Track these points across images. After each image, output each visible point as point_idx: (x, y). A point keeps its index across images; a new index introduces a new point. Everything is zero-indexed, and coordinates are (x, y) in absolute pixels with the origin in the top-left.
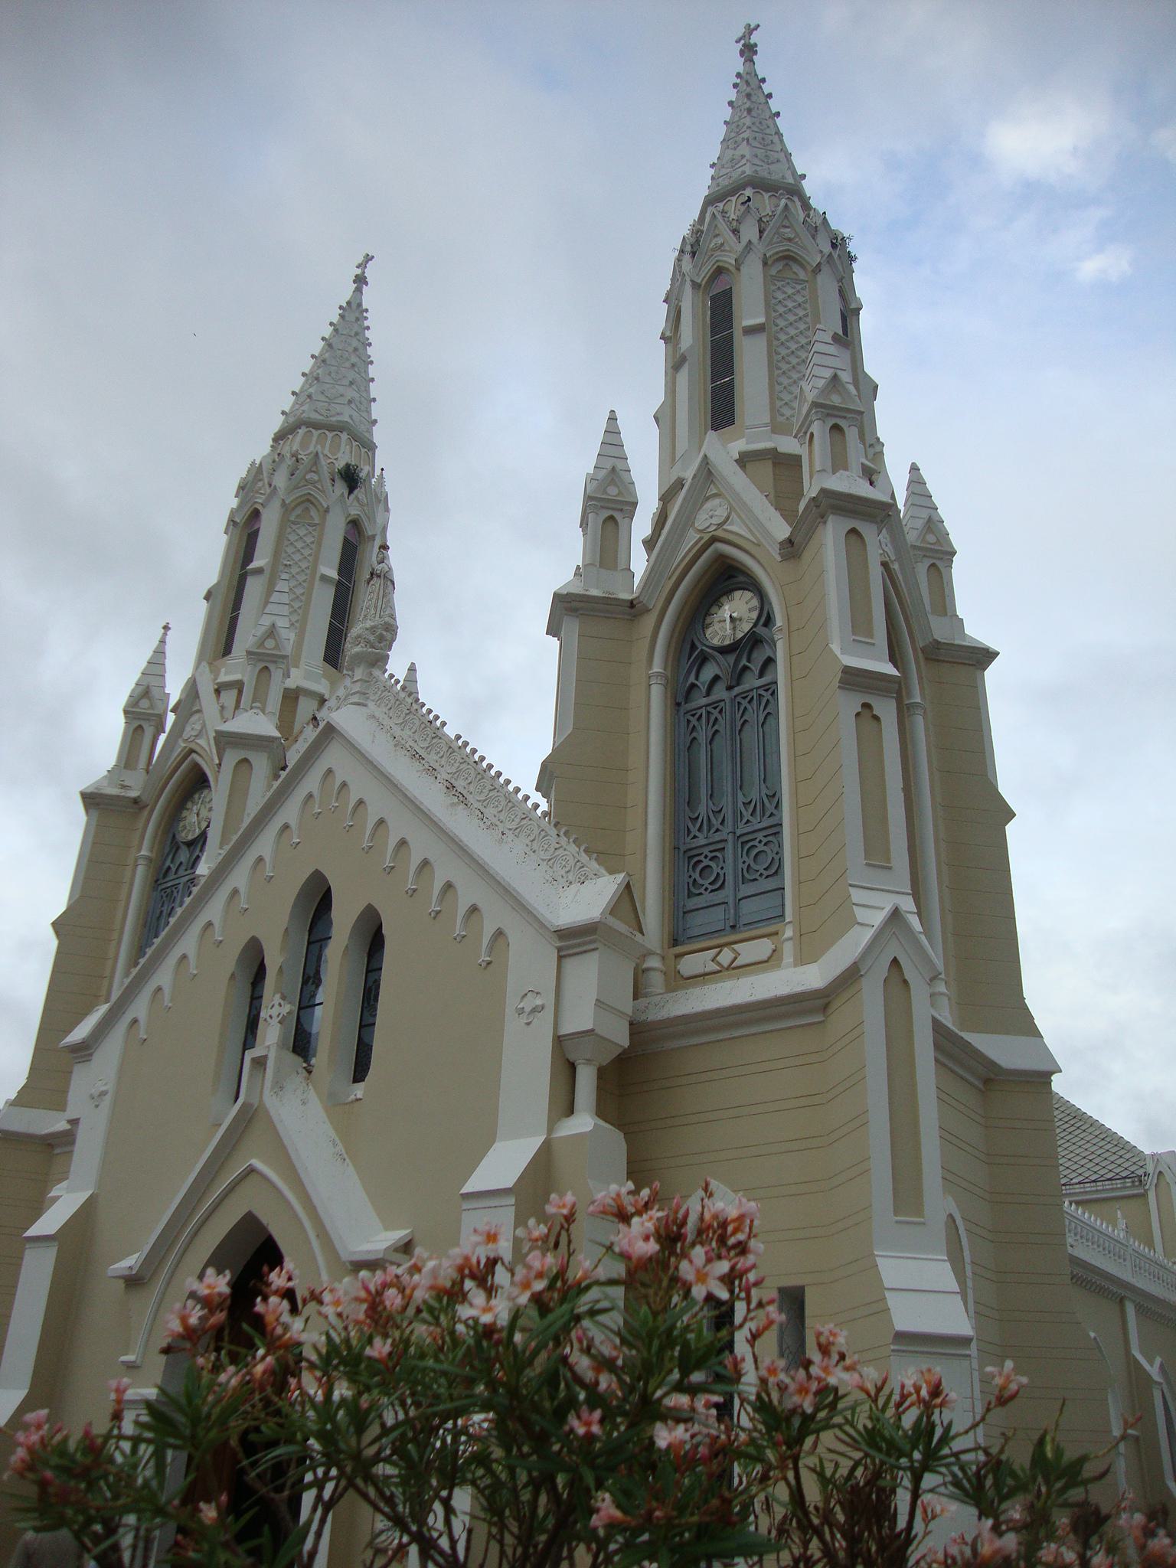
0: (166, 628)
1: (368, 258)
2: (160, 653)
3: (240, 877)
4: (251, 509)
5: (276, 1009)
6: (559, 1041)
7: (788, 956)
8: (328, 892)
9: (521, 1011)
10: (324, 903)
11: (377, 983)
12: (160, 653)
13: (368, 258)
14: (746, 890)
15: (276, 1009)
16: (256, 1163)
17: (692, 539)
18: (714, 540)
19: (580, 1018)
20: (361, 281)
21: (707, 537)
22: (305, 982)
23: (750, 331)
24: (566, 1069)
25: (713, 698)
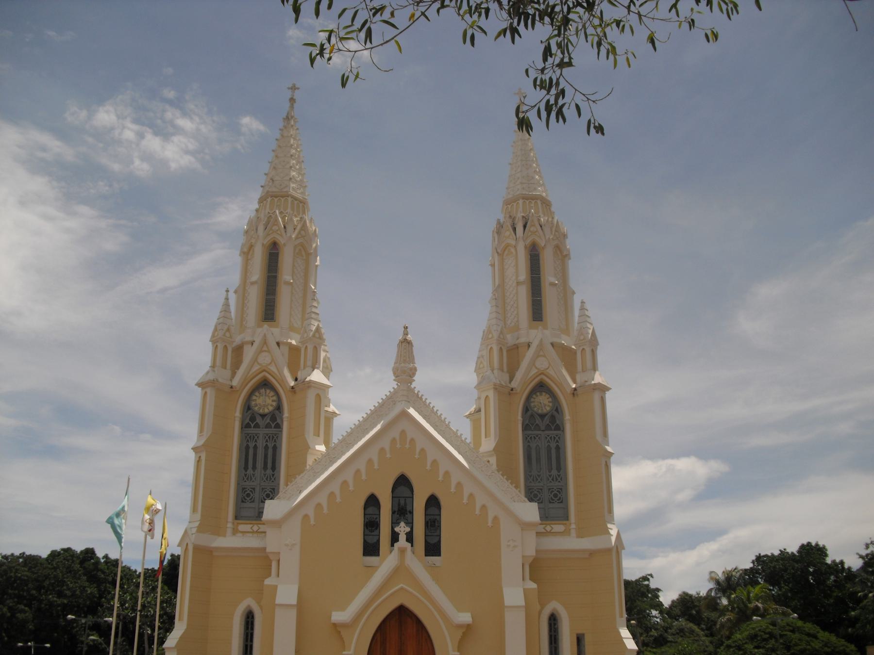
1: (294, 88)
2: (227, 305)
4: (272, 240)
7: (573, 533)
9: (509, 546)
12: (227, 305)
14: (551, 505)
18: (542, 373)
20: (292, 100)
21: (540, 373)
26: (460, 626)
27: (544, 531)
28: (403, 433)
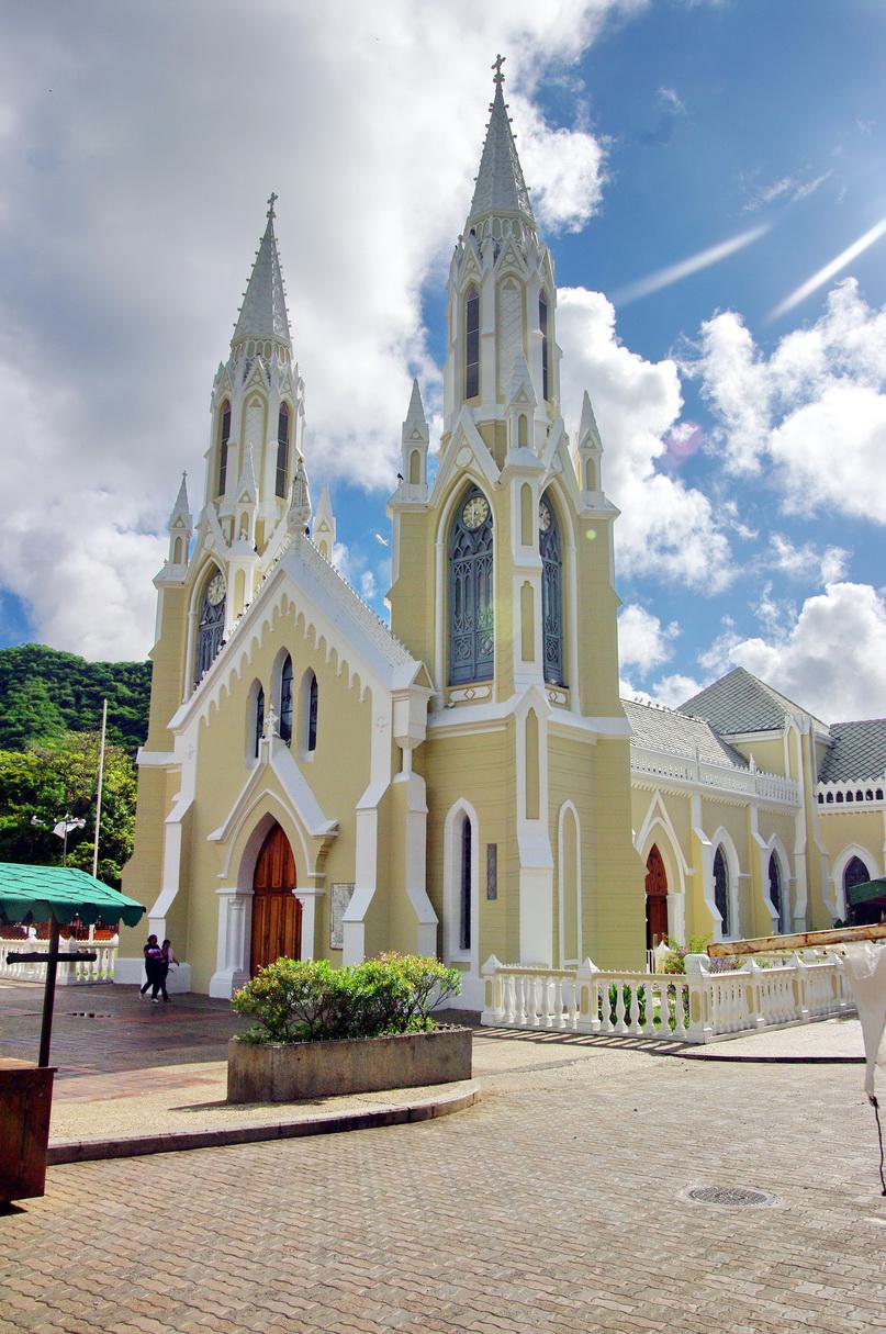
0: (185, 474)
1: (274, 197)
3: (246, 647)
5: (271, 720)
6: (394, 740)
8: (289, 657)
10: (288, 662)
11: (316, 703)
13: (274, 197)
15: (271, 720)
16: (269, 792)
17: (455, 471)
19: (402, 730)
20: (271, 215)
22: (283, 700)
23: (488, 335)
24: (398, 752)
25: (466, 558)
26: (317, 837)
27: (464, 698)
28: (285, 596)
